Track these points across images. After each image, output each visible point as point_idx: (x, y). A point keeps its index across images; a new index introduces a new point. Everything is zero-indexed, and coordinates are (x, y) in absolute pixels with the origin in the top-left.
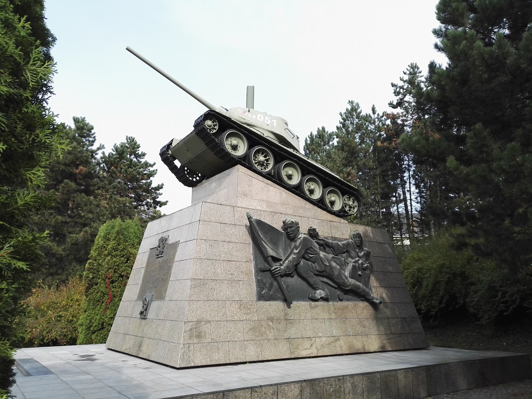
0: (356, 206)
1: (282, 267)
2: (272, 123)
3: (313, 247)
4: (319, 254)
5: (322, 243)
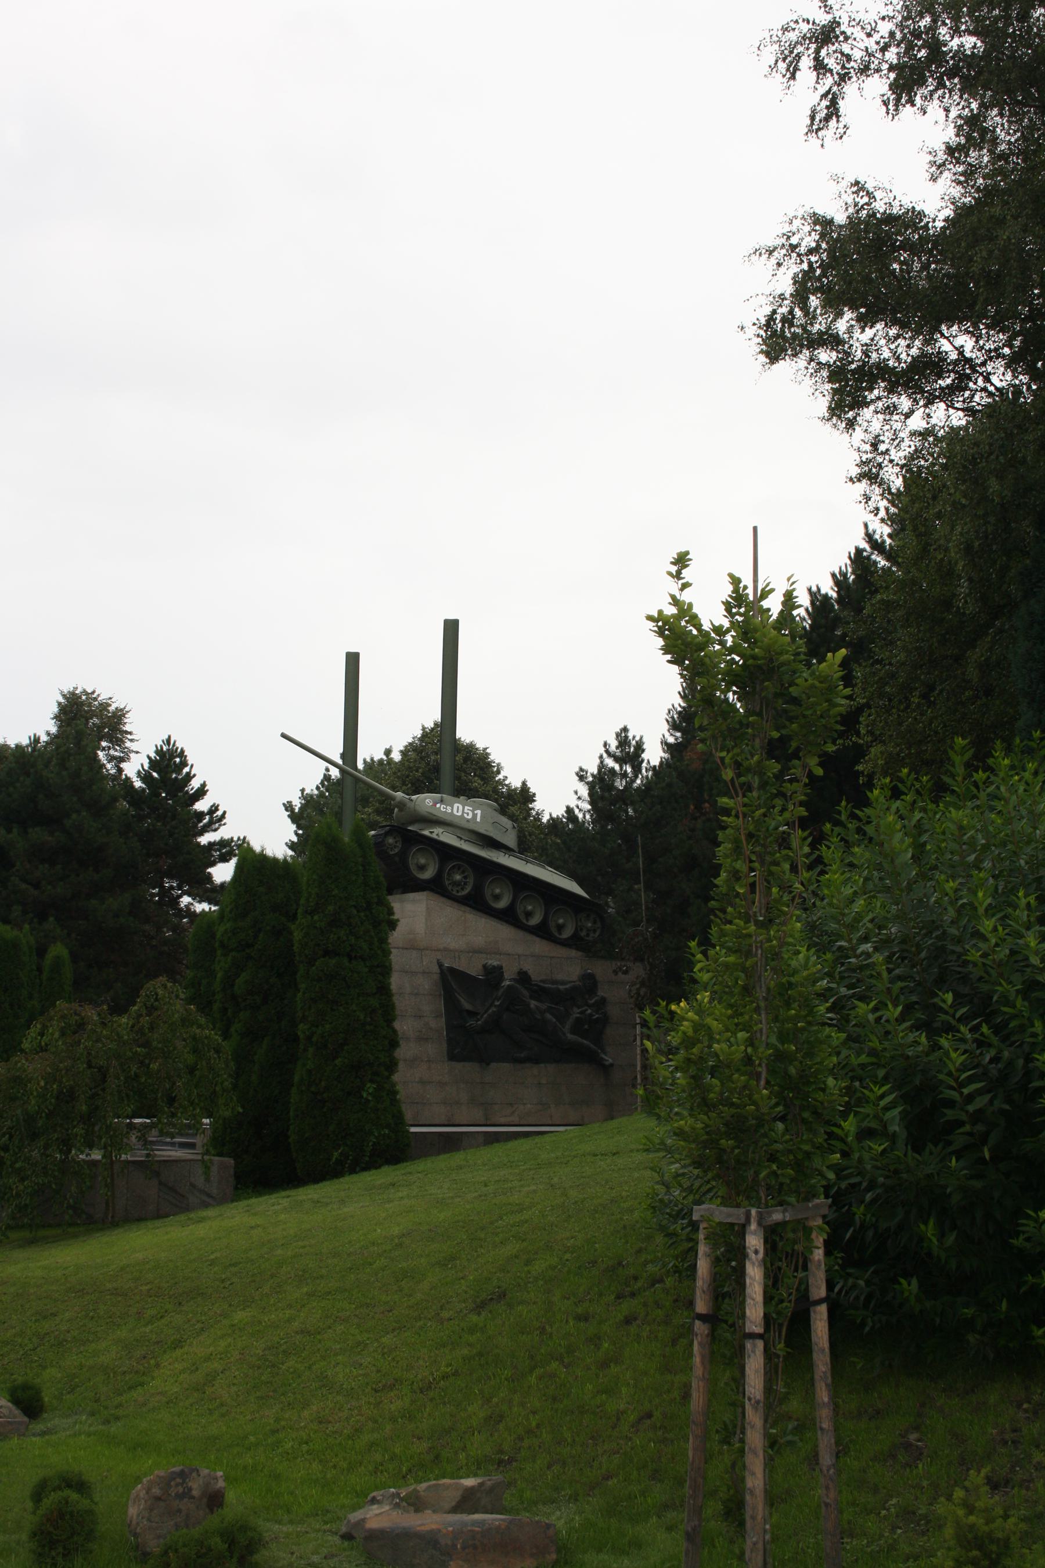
1: (479, 1022)
2: (475, 816)
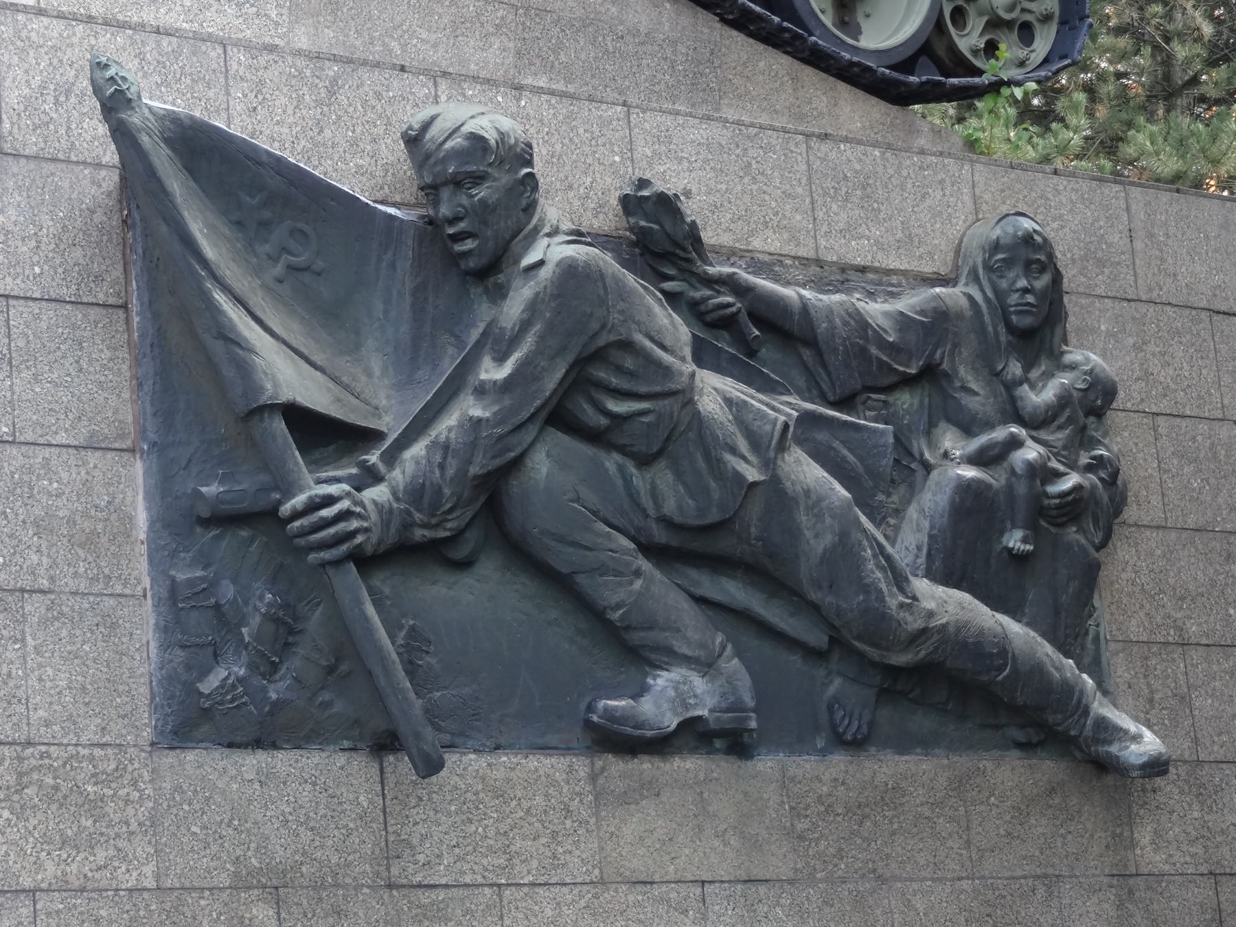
0: (1046, 19)
1: (377, 493)
3: (639, 338)
4: (686, 396)
5: (729, 305)
